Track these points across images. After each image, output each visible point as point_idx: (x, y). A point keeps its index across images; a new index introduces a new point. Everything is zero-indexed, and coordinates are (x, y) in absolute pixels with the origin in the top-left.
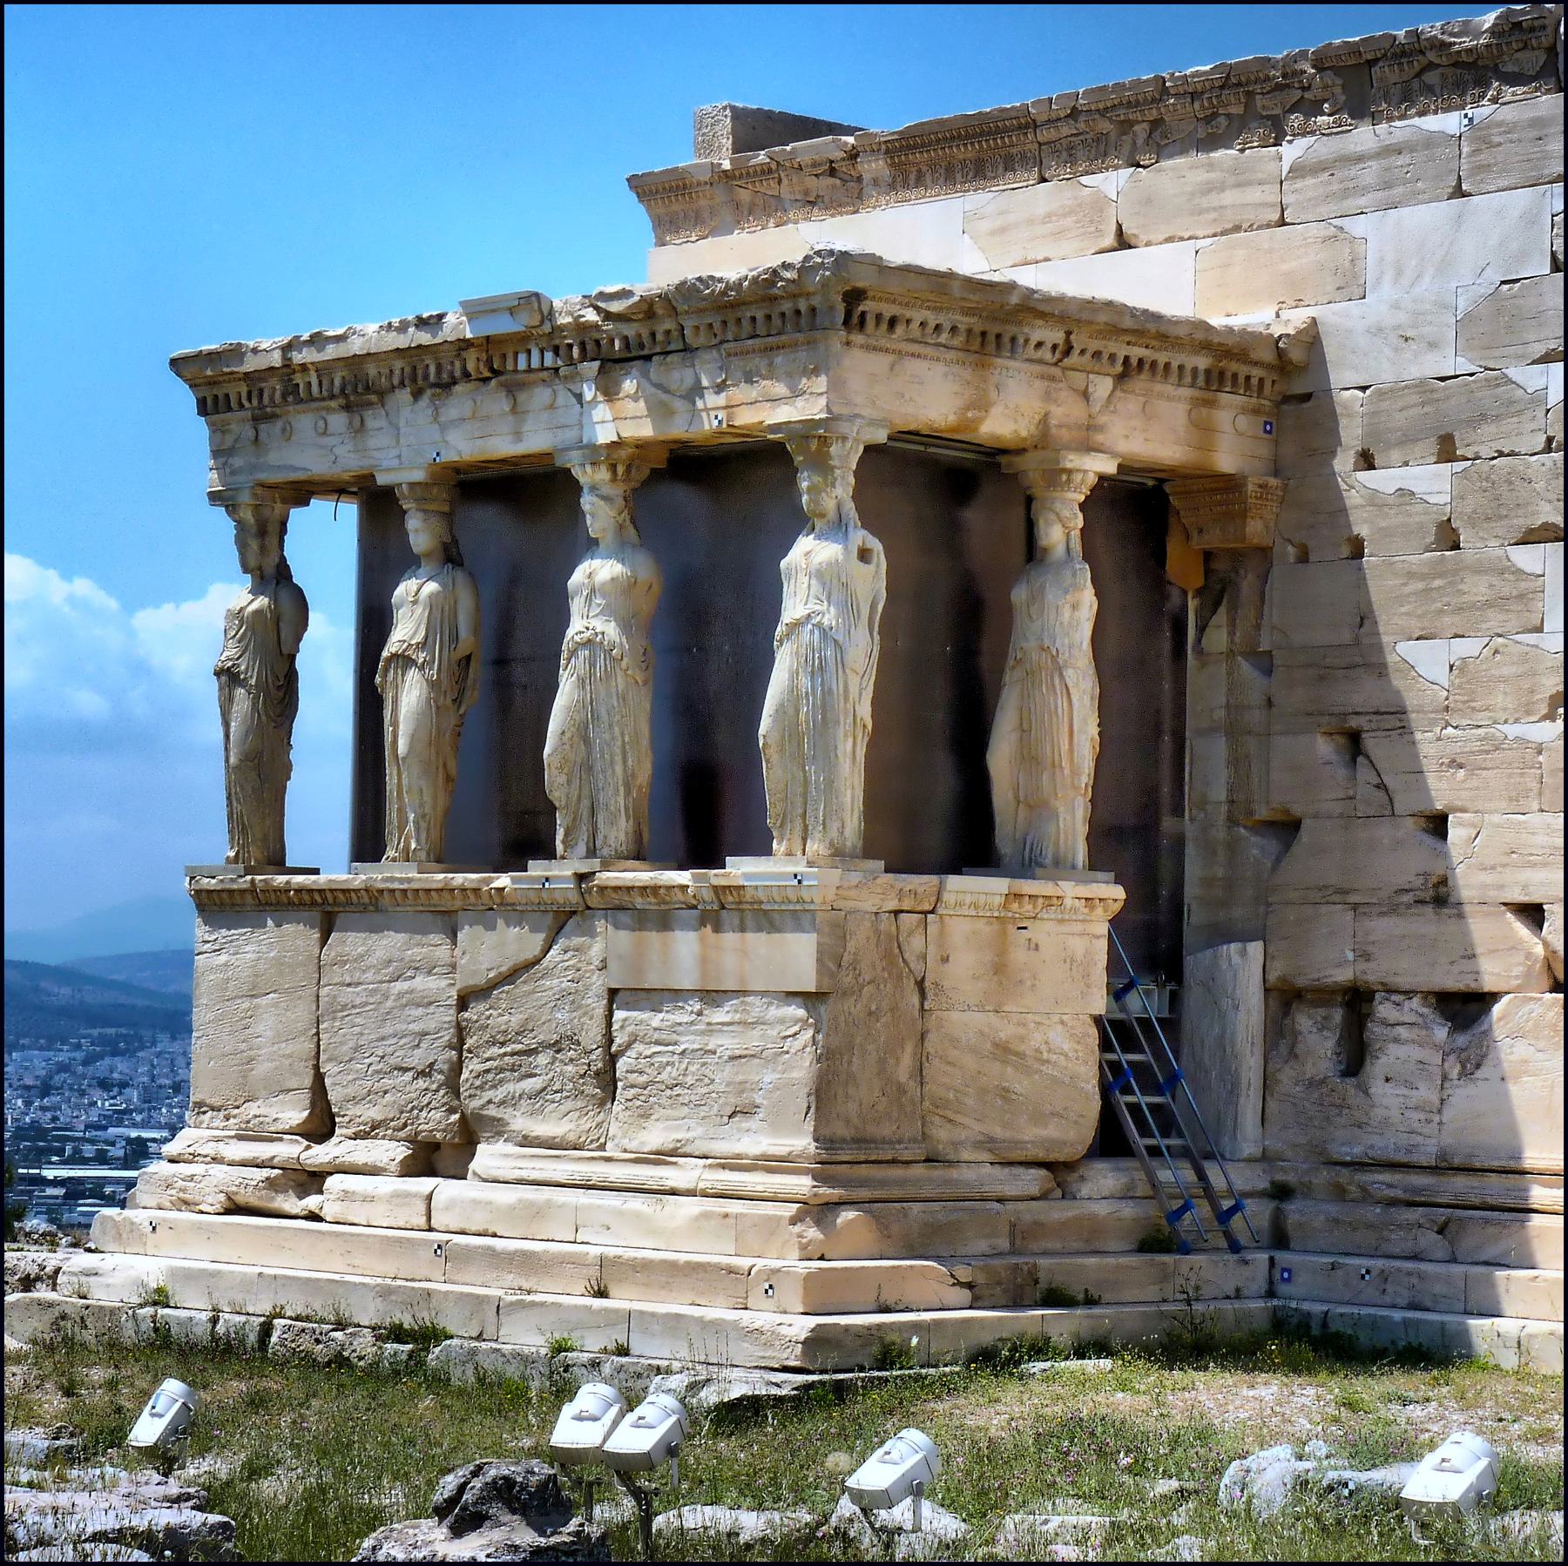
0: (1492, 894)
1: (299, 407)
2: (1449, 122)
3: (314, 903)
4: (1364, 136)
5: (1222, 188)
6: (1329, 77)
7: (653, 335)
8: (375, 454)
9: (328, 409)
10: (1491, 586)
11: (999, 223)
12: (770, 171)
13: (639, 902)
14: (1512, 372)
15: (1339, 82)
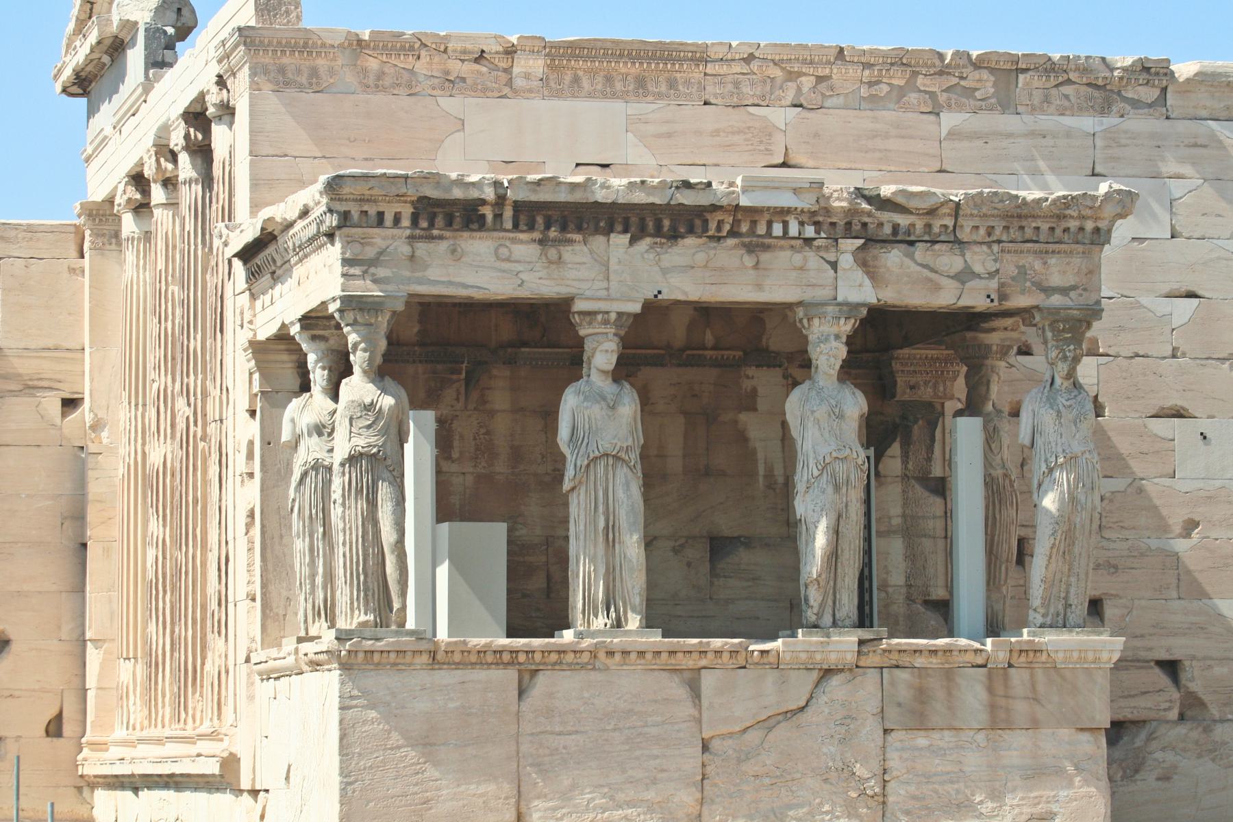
0: (1143, 654)
1: (478, 234)
2: (1088, 123)
3: (511, 664)
4: (1009, 122)
5: (886, 136)
6: (985, 75)
7: (928, 226)
8: (574, 283)
9: (514, 241)
10: (1132, 444)
11: (665, 129)
12: (412, 48)
13: (919, 661)
14: (1144, 300)
15: (992, 78)
